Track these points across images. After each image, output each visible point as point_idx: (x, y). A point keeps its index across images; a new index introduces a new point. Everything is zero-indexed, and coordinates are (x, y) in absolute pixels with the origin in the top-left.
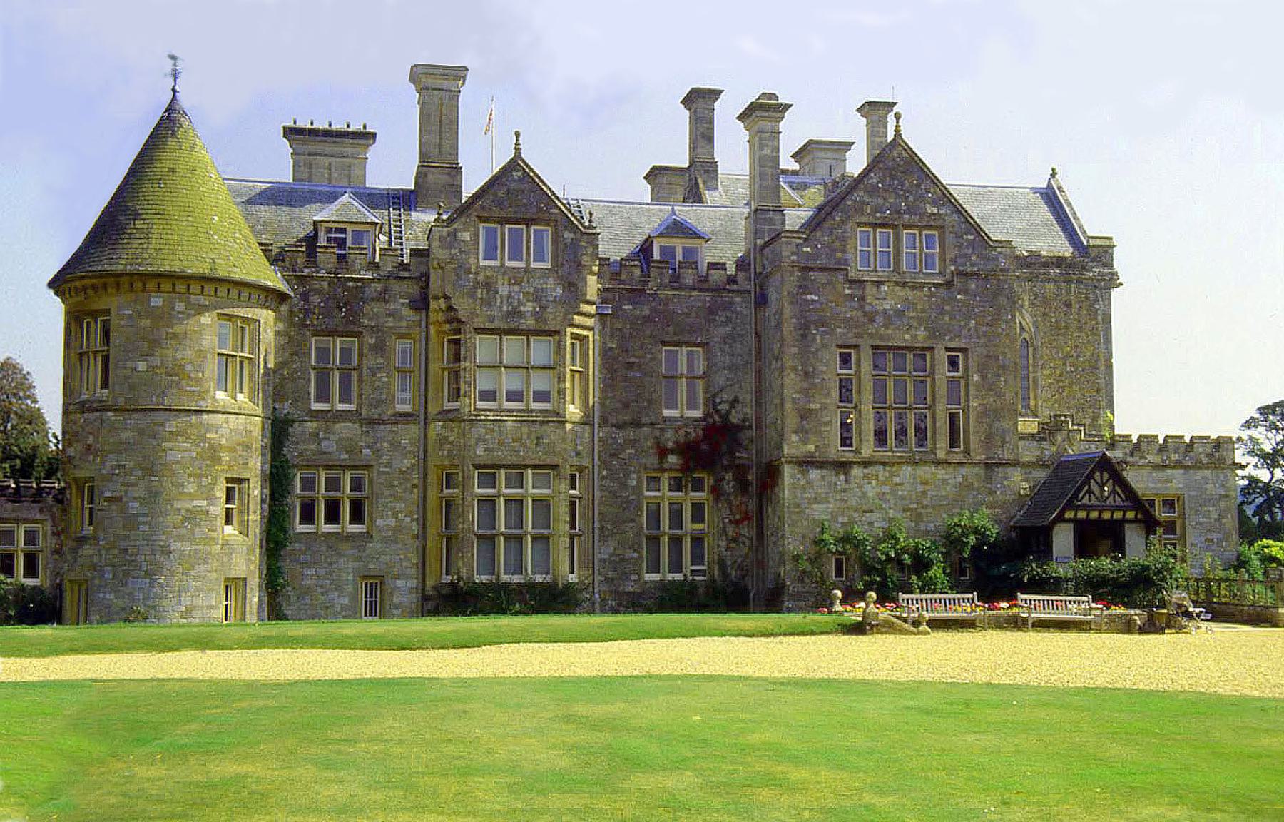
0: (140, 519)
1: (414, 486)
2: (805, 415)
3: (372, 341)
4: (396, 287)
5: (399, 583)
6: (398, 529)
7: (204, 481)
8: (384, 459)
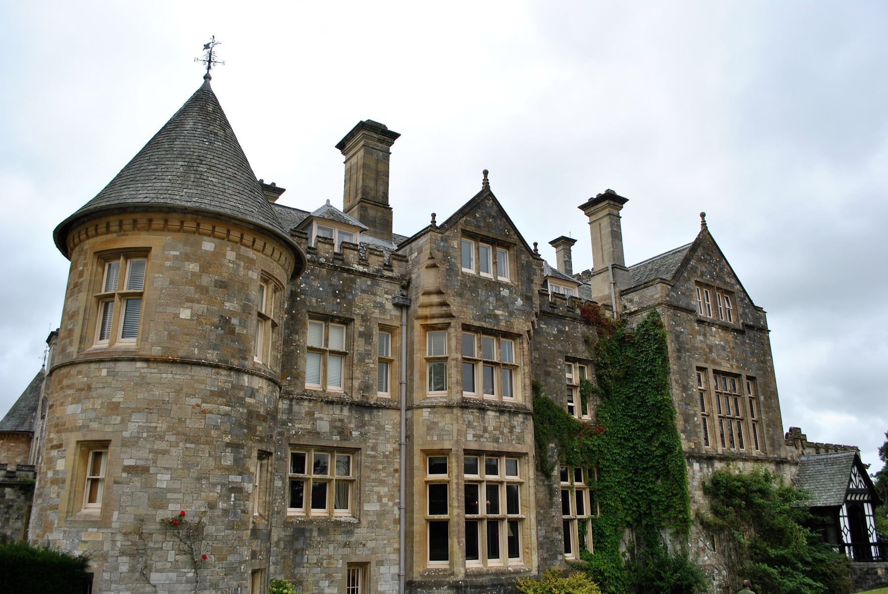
0: (169, 496)
1: (396, 471)
2: (687, 418)
3: (362, 329)
4: (385, 285)
5: (383, 569)
6: (382, 514)
7: (244, 451)
8: (371, 442)
